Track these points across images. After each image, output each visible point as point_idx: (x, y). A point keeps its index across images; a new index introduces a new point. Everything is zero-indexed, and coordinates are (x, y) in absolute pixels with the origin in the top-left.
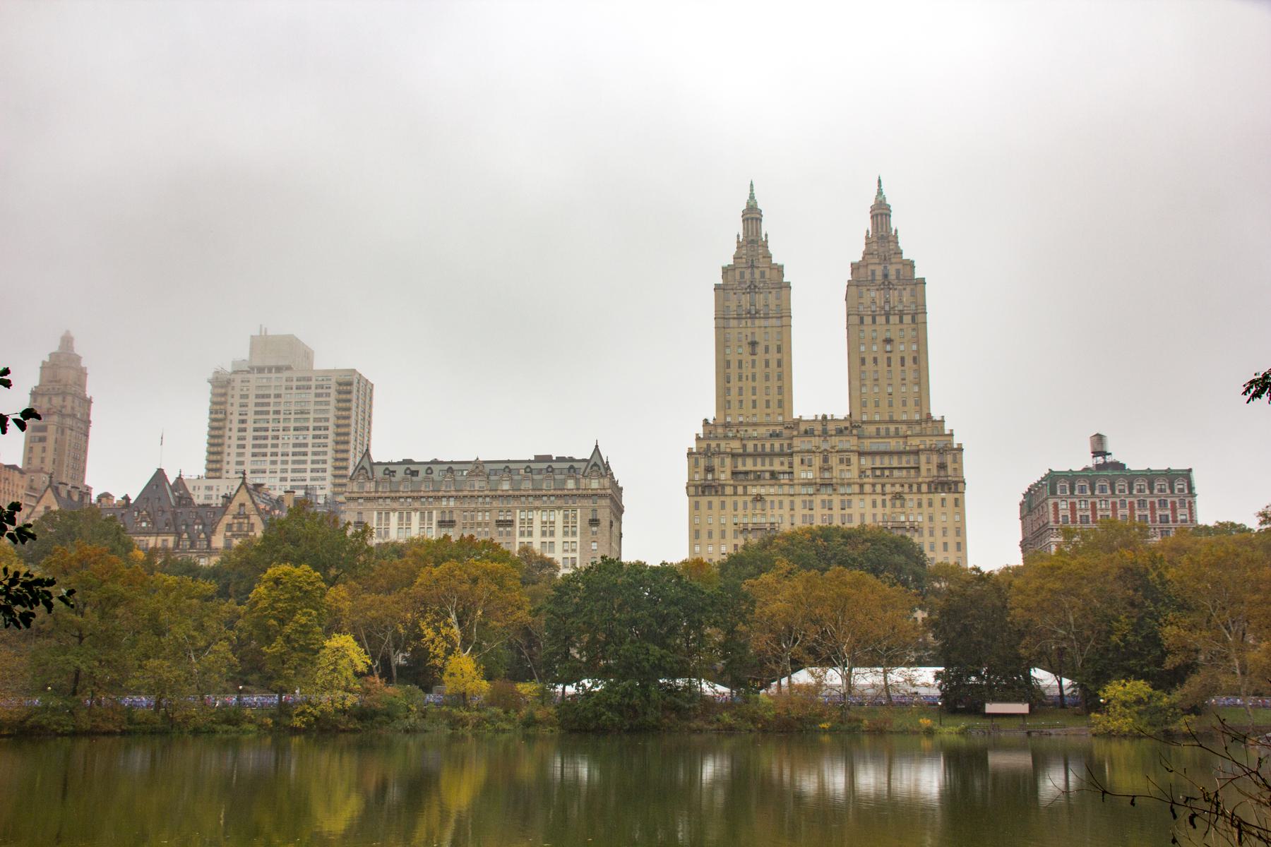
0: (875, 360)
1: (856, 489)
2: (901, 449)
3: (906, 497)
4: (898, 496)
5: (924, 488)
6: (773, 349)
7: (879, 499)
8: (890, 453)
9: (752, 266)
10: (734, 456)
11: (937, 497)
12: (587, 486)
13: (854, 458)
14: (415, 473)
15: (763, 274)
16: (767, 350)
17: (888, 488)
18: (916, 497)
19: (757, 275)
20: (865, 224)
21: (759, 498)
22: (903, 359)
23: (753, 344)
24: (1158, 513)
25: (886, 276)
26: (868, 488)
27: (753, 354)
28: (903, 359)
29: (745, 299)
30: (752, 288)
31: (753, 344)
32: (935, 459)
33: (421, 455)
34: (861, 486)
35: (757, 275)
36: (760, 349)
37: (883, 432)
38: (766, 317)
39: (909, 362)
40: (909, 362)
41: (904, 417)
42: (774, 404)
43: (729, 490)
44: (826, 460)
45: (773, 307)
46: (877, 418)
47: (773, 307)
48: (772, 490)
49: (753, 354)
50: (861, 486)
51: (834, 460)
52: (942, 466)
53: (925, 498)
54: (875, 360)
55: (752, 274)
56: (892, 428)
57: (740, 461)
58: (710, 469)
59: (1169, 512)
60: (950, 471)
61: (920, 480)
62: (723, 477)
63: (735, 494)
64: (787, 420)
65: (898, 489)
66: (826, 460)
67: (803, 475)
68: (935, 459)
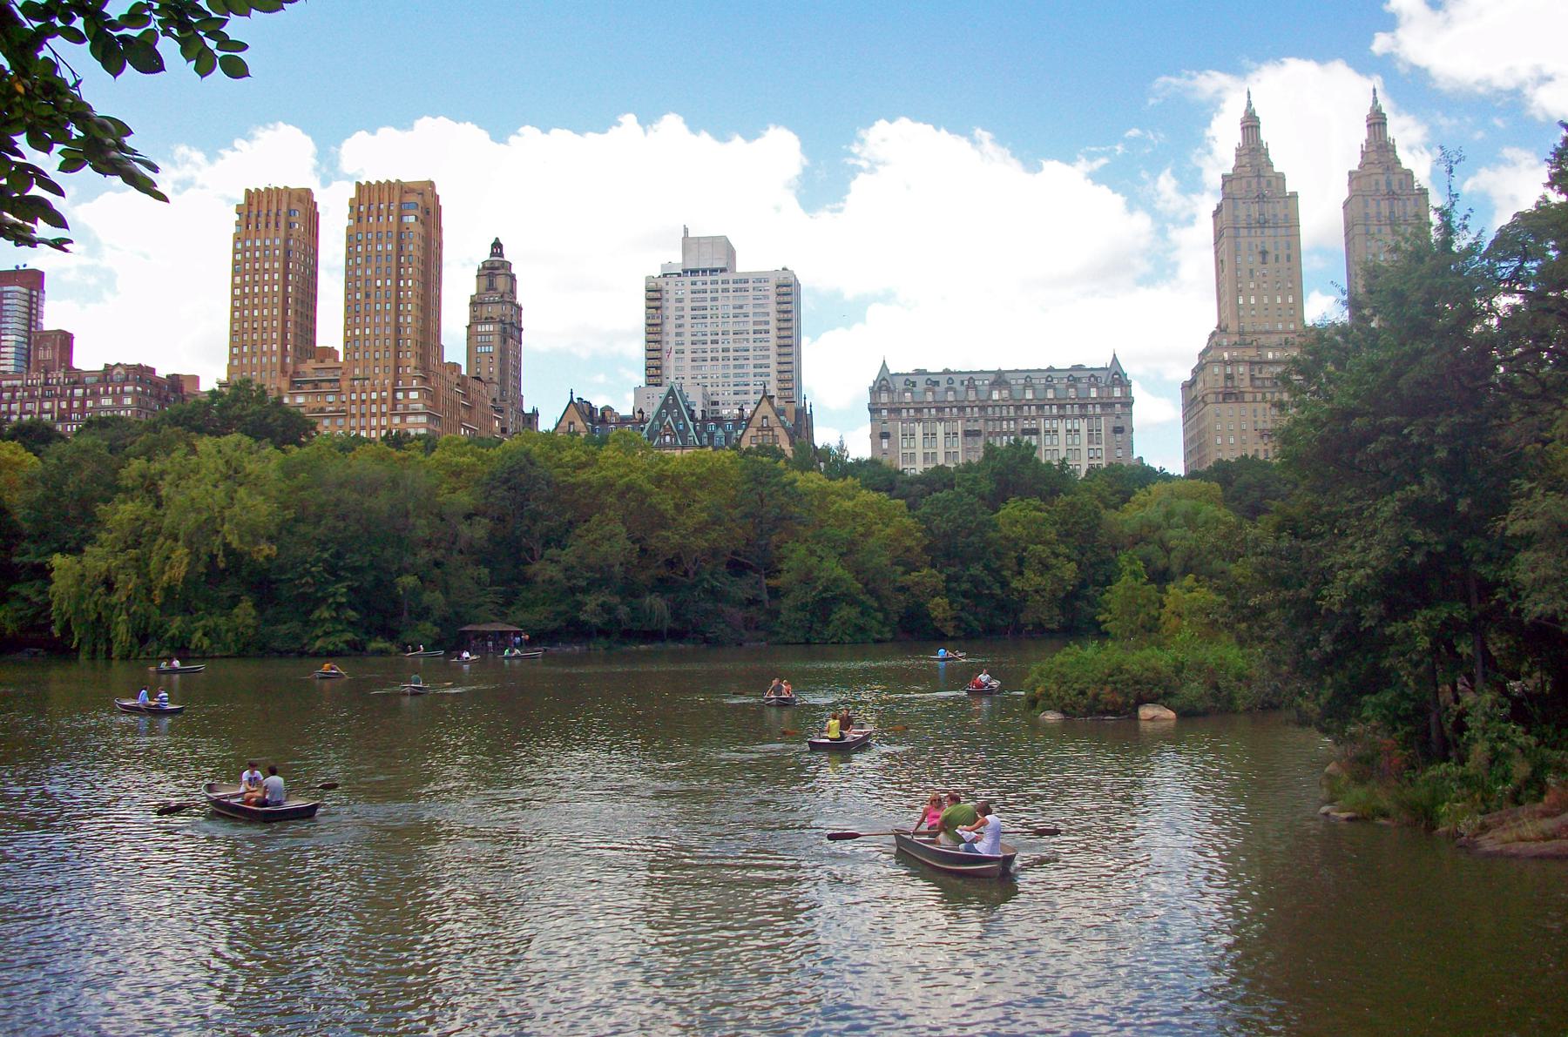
6: (1283, 258)
9: (1259, 176)
10: (1252, 363)
12: (1102, 393)
14: (937, 383)
19: (1264, 185)
20: (1361, 134)
23: (1264, 253)
25: (1389, 184)
27: (1264, 262)
29: (1254, 210)
30: (1261, 198)
31: (1264, 253)
33: (935, 366)
35: (1264, 185)
36: (1270, 258)
38: (1276, 227)
43: (1248, 397)
45: (1281, 216)
47: (1281, 216)
55: (1259, 183)
57: (1257, 368)
63: (1254, 401)
64: (1300, 328)
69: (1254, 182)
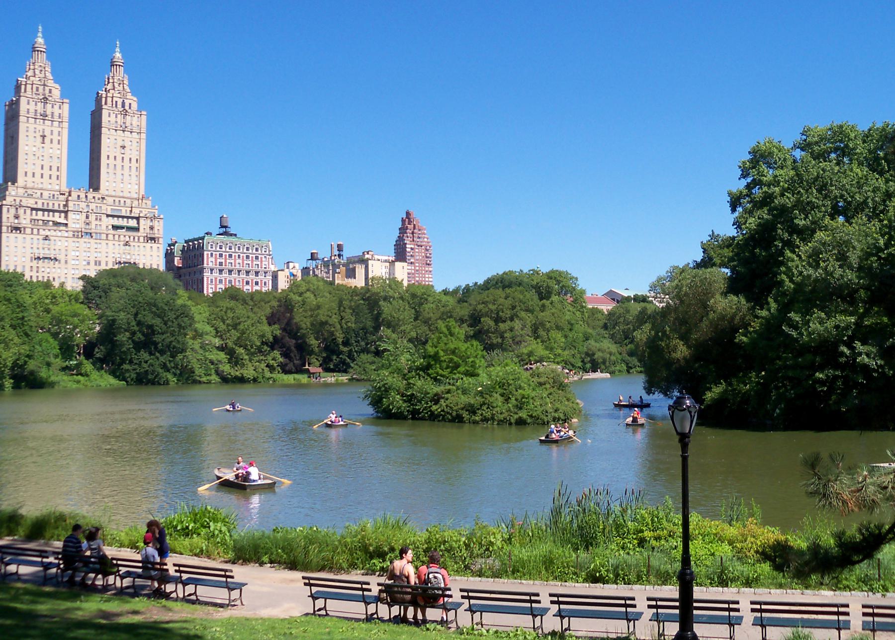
0: (115, 157)
1: (104, 236)
2: (128, 215)
3: (132, 244)
4: (127, 244)
5: (142, 239)
7: (117, 243)
8: (123, 217)
9: (44, 85)
11: (148, 245)
13: (104, 217)
15: (50, 91)
16: (51, 142)
17: (122, 238)
18: (136, 244)
19: (47, 92)
21: (46, 238)
22: (130, 159)
23: (44, 137)
24: (219, 261)
26: (110, 237)
28: (130, 159)
29: (40, 106)
31: (44, 137)
32: (149, 223)
34: (107, 235)
36: (47, 140)
37: (117, 204)
39: (134, 161)
40: (134, 161)
41: (129, 195)
42: (54, 177)
43: (28, 231)
44: (87, 217)
46: (114, 193)
48: (54, 233)
49: (43, 143)
50: (107, 235)
51: (92, 217)
52: (152, 228)
53: (142, 245)
54: (115, 157)
56: (122, 200)
58: (17, 217)
59: (223, 261)
60: (156, 231)
61: (139, 234)
62: (24, 222)
65: (127, 239)
66: (87, 217)
67: (74, 226)
68: (149, 223)
69: (41, 88)
